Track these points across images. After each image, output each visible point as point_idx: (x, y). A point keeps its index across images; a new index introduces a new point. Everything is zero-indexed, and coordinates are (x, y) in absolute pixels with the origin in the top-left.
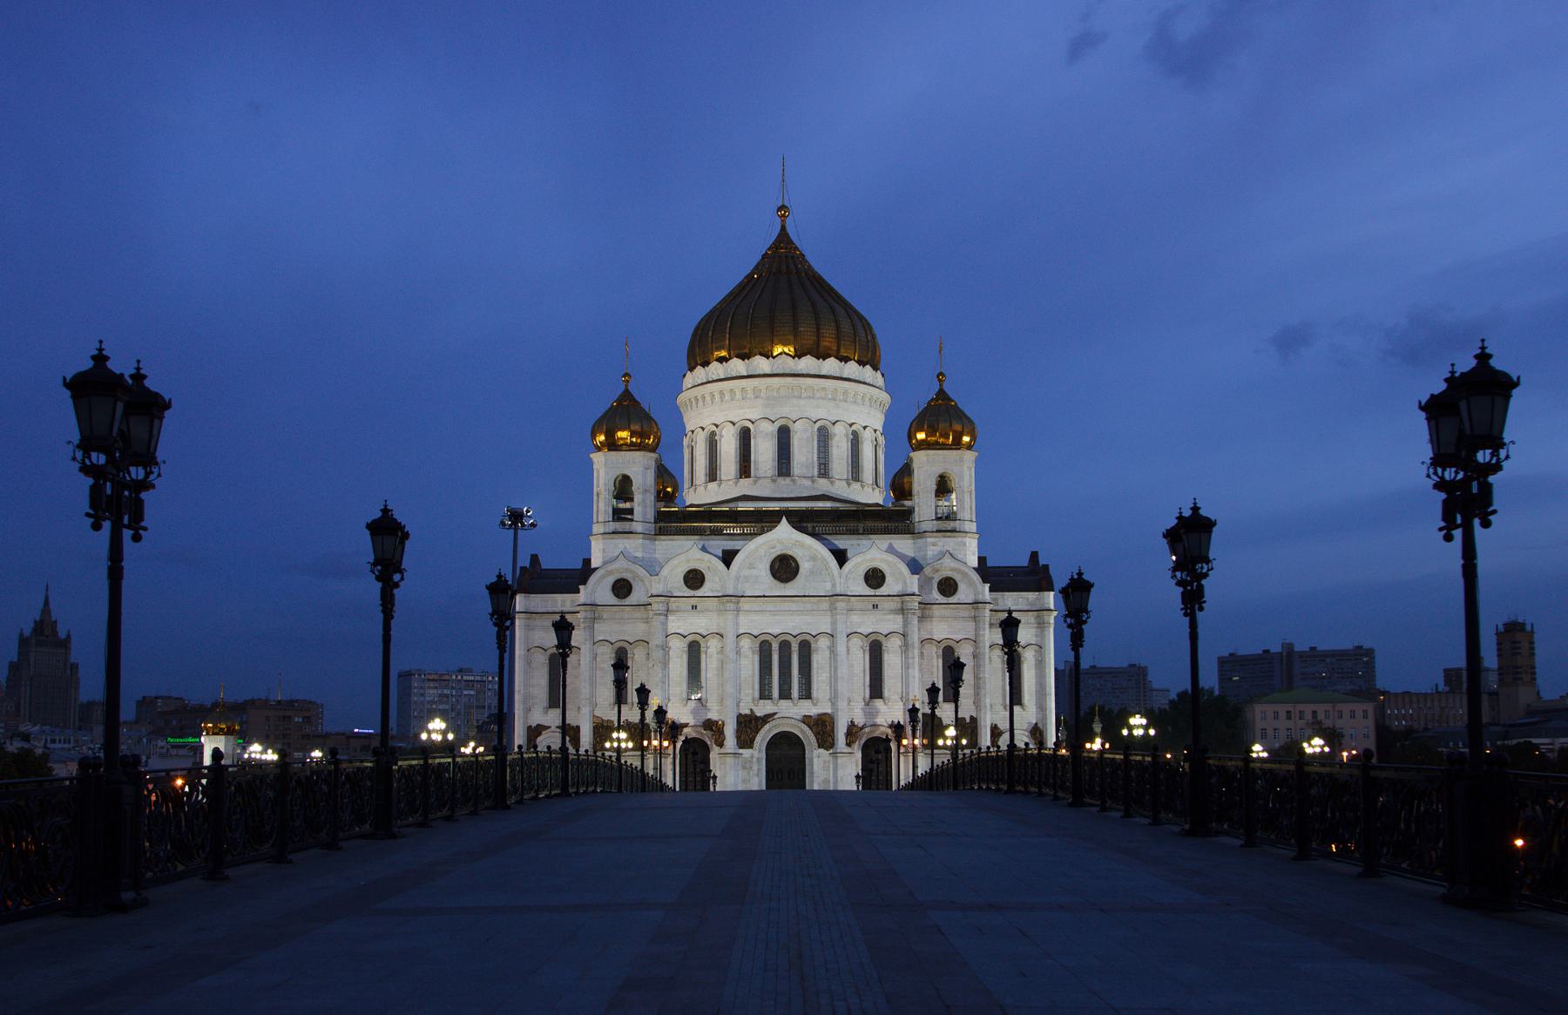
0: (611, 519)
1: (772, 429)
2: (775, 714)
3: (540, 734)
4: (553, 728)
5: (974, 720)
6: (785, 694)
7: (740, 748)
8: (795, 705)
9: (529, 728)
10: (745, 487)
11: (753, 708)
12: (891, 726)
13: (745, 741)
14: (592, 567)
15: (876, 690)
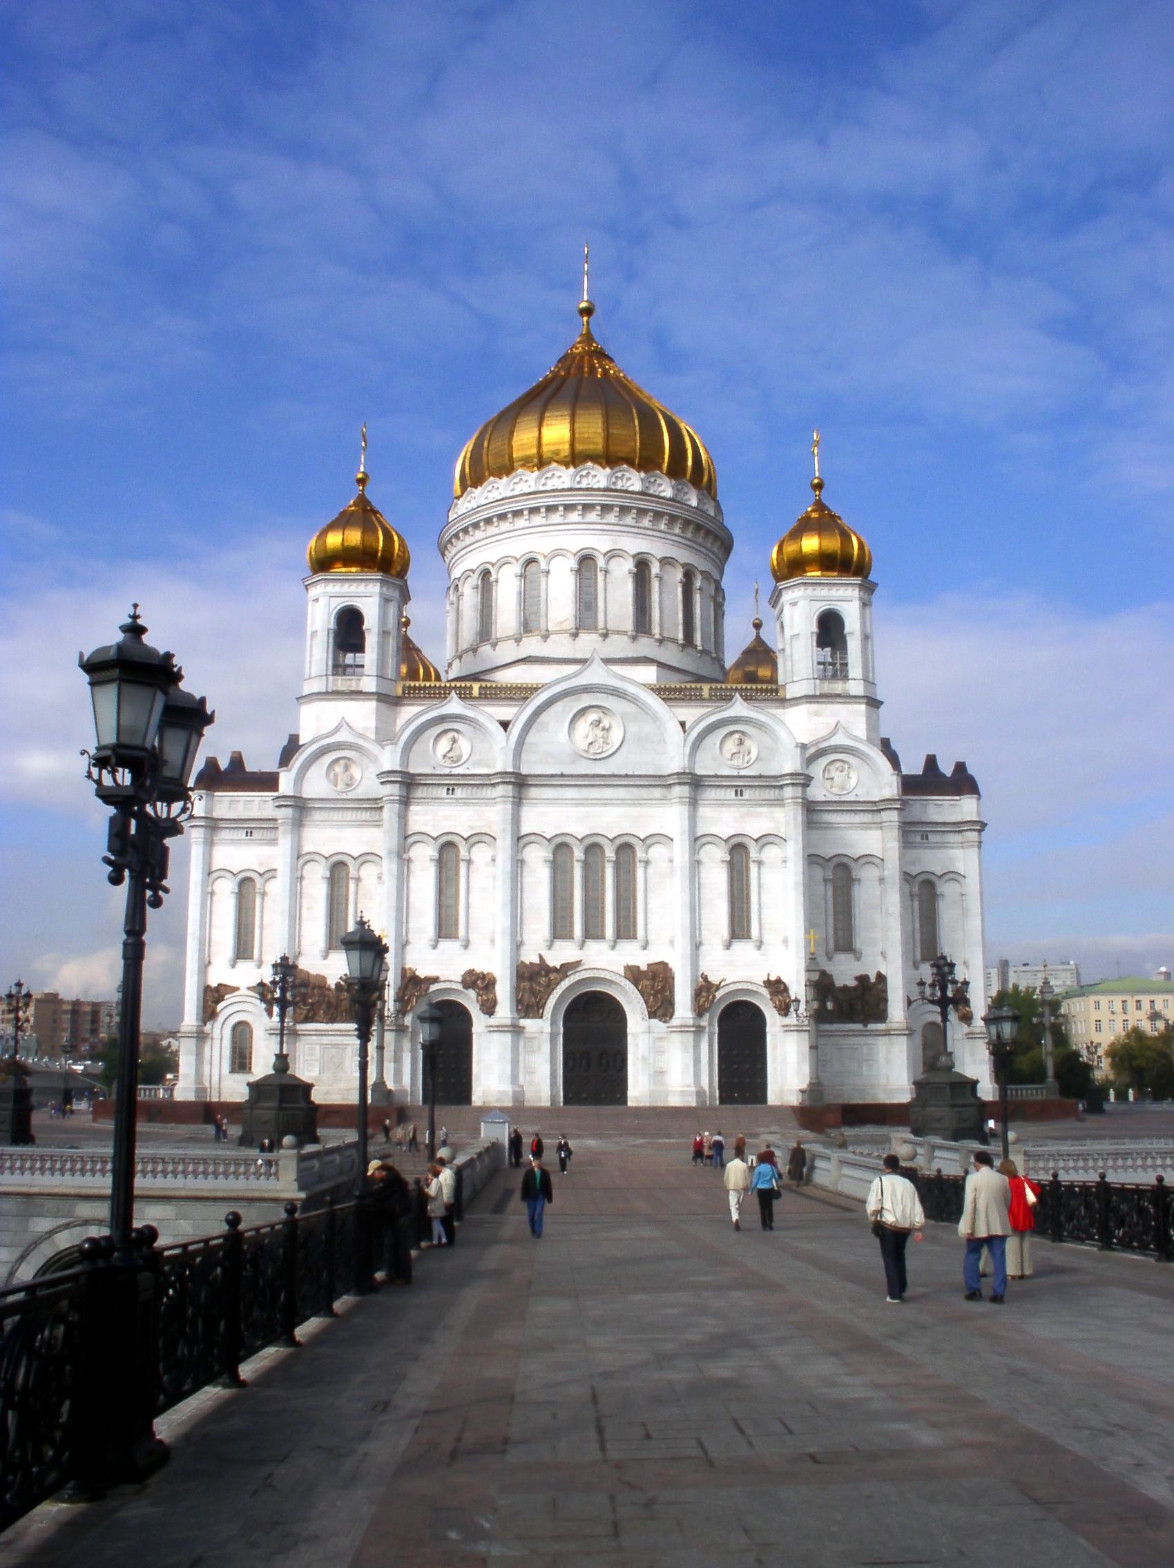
0: (330, 672)
1: (572, 563)
2: (578, 963)
3: (220, 999)
4: (243, 991)
5: (881, 978)
6: (593, 932)
7: (526, 1016)
8: (613, 948)
9: (207, 989)
10: (533, 646)
11: (542, 954)
12: (768, 984)
13: (528, 1005)
14: (301, 743)
15: (739, 928)
